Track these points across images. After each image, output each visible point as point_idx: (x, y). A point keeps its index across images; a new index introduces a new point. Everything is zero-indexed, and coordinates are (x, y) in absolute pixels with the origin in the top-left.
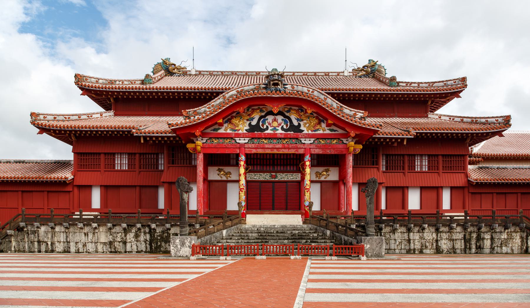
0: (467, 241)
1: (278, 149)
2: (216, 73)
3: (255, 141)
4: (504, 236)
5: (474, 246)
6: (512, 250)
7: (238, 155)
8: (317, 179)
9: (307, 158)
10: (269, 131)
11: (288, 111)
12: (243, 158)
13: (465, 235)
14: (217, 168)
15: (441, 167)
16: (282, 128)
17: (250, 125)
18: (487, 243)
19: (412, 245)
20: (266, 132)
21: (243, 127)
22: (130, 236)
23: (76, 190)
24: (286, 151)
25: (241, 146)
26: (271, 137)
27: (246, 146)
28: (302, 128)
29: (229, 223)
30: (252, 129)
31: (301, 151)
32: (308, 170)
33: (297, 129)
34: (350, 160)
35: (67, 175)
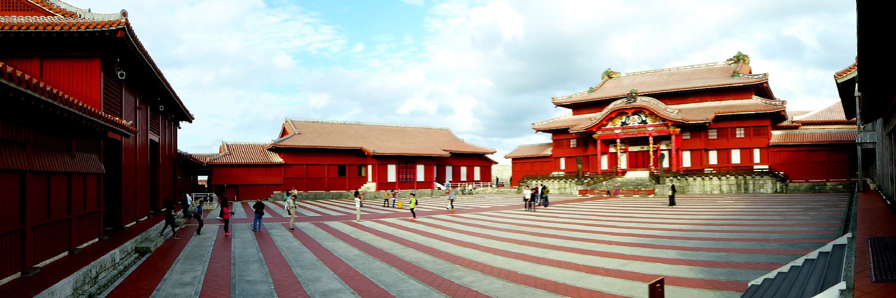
0: (739, 186)
1: (635, 134)
2: (637, 73)
3: (625, 131)
4: (761, 182)
5: (743, 189)
6: (767, 191)
7: (616, 140)
8: (666, 148)
9: (651, 138)
10: (630, 125)
11: (640, 113)
12: (618, 141)
13: (737, 182)
14: (613, 145)
15: (752, 134)
16: (638, 123)
17: (622, 122)
18: (751, 187)
19: (706, 188)
20: (629, 125)
21: (618, 122)
22: (568, 184)
23: (554, 159)
24: (640, 136)
25: (617, 134)
26: (633, 128)
27: (620, 134)
28: (647, 121)
29: (607, 178)
30: (624, 124)
31: (647, 135)
32: (651, 146)
33: (644, 122)
34: (673, 138)
35: (549, 152)
